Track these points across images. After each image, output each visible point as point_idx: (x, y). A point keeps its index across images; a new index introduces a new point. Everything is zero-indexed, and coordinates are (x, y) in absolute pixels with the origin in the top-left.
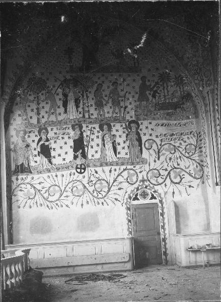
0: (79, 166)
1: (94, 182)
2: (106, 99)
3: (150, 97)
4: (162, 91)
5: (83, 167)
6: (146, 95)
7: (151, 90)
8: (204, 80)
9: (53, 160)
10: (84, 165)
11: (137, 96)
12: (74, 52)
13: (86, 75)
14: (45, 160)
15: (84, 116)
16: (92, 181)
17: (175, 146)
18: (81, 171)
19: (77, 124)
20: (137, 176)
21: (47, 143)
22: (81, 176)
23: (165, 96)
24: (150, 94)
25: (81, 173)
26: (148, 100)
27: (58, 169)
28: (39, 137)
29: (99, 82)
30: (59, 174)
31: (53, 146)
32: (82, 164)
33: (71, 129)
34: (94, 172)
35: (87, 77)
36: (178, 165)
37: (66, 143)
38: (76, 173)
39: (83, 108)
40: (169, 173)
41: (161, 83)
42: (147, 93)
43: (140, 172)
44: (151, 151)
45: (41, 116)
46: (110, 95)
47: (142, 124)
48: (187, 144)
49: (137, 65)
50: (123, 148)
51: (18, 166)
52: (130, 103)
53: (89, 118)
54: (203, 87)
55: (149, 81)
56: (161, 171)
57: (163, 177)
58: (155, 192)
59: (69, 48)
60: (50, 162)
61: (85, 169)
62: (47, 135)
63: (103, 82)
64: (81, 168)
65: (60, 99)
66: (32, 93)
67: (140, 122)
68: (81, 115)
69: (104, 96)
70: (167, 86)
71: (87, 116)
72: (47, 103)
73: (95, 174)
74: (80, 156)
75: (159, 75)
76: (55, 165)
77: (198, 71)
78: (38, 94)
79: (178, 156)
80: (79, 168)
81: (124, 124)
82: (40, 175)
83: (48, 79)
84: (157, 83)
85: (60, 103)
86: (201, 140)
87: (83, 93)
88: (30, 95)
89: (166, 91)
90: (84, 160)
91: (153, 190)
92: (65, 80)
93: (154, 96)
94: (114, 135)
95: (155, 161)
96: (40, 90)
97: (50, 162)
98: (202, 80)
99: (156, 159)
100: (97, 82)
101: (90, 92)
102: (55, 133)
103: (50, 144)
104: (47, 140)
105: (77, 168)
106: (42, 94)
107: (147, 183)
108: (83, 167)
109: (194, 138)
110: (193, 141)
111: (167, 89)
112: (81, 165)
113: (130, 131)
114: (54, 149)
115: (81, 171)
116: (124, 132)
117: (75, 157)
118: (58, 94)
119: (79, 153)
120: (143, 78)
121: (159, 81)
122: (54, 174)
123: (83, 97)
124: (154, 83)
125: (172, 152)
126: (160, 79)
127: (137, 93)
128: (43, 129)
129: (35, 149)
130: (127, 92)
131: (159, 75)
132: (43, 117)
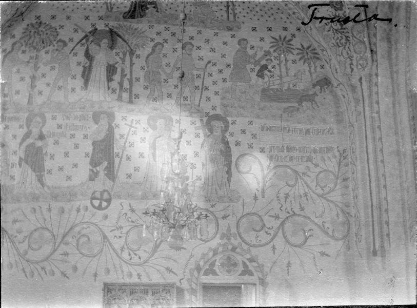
0: (98, 195)
1: (125, 230)
2: (168, 70)
3: (254, 75)
4: (277, 67)
7: (256, 63)
8: (354, 58)
9: (49, 180)
11: (227, 73)
13: (136, 26)
14: (31, 176)
16: (121, 228)
17: (296, 172)
19: (104, 113)
20: (218, 225)
21: (39, 143)
22: (101, 213)
23: (281, 77)
24: (252, 70)
25: (100, 208)
27: (55, 197)
28: (25, 130)
29: (158, 39)
30: (56, 205)
31: (50, 149)
32: (105, 191)
33: (91, 119)
34: (126, 208)
36: (302, 209)
37: (77, 147)
39: (121, 84)
40: (283, 224)
41: (276, 54)
42: (249, 67)
43: (224, 217)
46: (176, 63)
47: (234, 122)
49: (231, 17)
52: (215, 83)
55: (252, 47)
56: (266, 218)
57: (269, 231)
58: (252, 260)
60: (40, 180)
61: (109, 201)
62: (43, 126)
63: (166, 41)
64: (101, 199)
65: (79, 64)
66: (27, 49)
67: (230, 119)
72: (53, 68)
74: (102, 174)
76: (48, 187)
78: (38, 51)
83: (62, 27)
84: (267, 53)
86: (347, 165)
87: (125, 54)
88: (24, 52)
89: (284, 70)
90: (109, 183)
91: (248, 256)
92: (94, 31)
97: (40, 180)
98: (351, 58)
100: (152, 40)
101: (138, 56)
102: (60, 126)
104: (41, 137)
105: (93, 198)
106: (47, 52)
107: (235, 242)
108: (106, 196)
109: (333, 160)
110: (332, 165)
111: (286, 65)
112: (102, 193)
114: (52, 157)
117: (93, 176)
118: (75, 54)
119: (101, 169)
121: (272, 50)
124: (263, 53)
125: (291, 183)
126: (272, 47)
127: (228, 66)
128: (36, 115)
129: (15, 152)
130: (209, 62)
131: (273, 40)
132: (40, 93)
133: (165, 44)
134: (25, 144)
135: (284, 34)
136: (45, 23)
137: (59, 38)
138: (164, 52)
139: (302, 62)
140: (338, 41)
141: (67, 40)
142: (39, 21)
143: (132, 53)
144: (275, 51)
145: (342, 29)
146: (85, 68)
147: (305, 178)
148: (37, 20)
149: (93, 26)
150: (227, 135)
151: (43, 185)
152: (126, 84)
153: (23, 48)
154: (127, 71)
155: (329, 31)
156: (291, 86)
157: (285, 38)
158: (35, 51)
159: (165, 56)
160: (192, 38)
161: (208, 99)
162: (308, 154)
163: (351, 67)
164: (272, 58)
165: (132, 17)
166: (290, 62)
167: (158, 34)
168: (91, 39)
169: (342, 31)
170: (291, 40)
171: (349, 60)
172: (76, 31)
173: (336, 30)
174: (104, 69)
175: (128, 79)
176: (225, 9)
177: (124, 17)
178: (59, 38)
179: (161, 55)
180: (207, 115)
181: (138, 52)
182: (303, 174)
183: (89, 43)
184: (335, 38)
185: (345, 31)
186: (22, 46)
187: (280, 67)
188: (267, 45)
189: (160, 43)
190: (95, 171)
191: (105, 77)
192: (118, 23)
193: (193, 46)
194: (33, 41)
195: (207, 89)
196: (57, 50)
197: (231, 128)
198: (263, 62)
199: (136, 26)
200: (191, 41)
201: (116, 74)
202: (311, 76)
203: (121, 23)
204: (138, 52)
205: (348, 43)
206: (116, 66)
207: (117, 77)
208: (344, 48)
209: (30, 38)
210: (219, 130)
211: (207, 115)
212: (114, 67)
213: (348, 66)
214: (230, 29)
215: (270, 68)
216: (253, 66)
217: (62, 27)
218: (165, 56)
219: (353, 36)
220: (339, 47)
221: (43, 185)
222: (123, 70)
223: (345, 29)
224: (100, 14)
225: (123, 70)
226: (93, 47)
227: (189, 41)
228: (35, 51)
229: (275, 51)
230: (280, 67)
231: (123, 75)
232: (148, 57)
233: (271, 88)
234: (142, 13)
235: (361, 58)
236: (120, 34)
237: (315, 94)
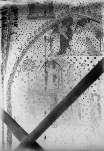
2: (76, 75)
12: (54, 41)
13: (62, 57)
15: (58, 88)
28: (28, 100)
29: (72, 63)
35: (63, 59)
39: (58, 82)
50: (86, 114)
53: (62, 89)
59: (50, 38)
62: (34, 99)
68: (57, 87)
71: (60, 87)
87: (59, 70)
94: (79, 104)
96: (31, 68)
100: (69, 63)
101: (64, 71)
106: (32, 71)
123: (59, 73)
133: (74, 65)
134: (29, 105)
136: (30, 60)
137: (35, 65)
138: (74, 68)
141: (38, 66)
142: (28, 59)
143: (62, 69)
150: (100, 102)
152: (60, 83)
154: (60, 77)
159: (74, 69)
160: (85, 61)
165: (61, 54)
174: (52, 76)
175: (61, 80)
177: (58, 54)
178: (35, 65)
181: (64, 69)
183: (46, 67)
189: (72, 65)
191: (53, 80)
193: (85, 64)
196: (35, 70)
199: (62, 57)
200: (85, 62)
201: (56, 78)
203: (57, 57)
204: (64, 69)
206: (56, 75)
207: (57, 80)
209: (26, 66)
210: (96, 100)
211: (92, 94)
212: (55, 76)
217: (35, 61)
222: (59, 77)
224: (48, 54)
225: (59, 77)
226: (47, 68)
227: (84, 62)
231: (59, 79)
232: (68, 71)
234: (65, 52)
236: (57, 62)
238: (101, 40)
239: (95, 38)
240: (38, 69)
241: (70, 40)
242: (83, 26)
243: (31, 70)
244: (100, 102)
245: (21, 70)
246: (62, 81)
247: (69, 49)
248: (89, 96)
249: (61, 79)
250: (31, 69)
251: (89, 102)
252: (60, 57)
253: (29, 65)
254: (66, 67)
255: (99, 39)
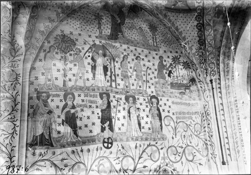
0: (106, 140)
1: (121, 159)
2: (131, 70)
4: (175, 72)
5: (110, 141)
6: (163, 73)
7: (167, 69)
9: (80, 133)
10: (111, 139)
12: (103, 19)
13: (114, 44)
14: (69, 130)
15: (111, 86)
18: (108, 145)
19: (105, 93)
20: (159, 153)
22: (108, 151)
24: (166, 73)
25: (108, 148)
26: (164, 78)
27: (84, 143)
28: (64, 103)
29: (125, 53)
31: (79, 115)
33: (99, 97)
34: (120, 148)
35: (114, 46)
36: (191, 143)
37: (93, 113)
38: (103, 148)
39: (111, 77)
40: (184, 150)
41: (174, 65)
42: (165, 71)
43: (162, 149)
44: (169, 127)
45: (67, 79)
46: (134, 67)
48: (195, 123)
50: (147, 123)
51: (37, 137)
52: (151, 79)
53: (116, 88)
54: (207, 75)
55: (165, 61)
56: (178, 148)
57: (180, 154)
58: (174, 170)
60: (75, 133)
61: (112, 143)
62: (73, 101)
64: (108, 143)
65: (89, 64)
66: (59, 51)
67: (159, 98)
68: (109, 84)
69: (129, 68)
70: (179, 69)
71: (114, 84)
72: (75, 65)
73: (122, 150)
74: (107, 128)
75: (173, 58)
76: (80, 137)
77: (203, 61)
79: (190, 134)
80: (106, 142)
81: (146, 98)
82: (63, 150)
84: (171, 65)
85: (89, 68)
86: (204, 121)
88: (57, 53)
90: (111, 133)
91: (173, 168)
93: (169, 76)
94: (138, 109)
95: (173, 138)
96: (69, 50)
97: (75, 133)
99: (174, 136)
101: (117, 62)
102: (83, 101)
103: (77, 112)
104: (73, 107)
105: (104, 142)
106: (71, 55)
107: (167, 161)
108: (110, 141)
110: (199, 120)
111: (178, 71)
112: (108, 139)
113: (151, 105)
114: (81, 119)
115: (108, 145)
116: (147, 106)
117: (103, 129)
119: (106, 125)
120: (161, 58)
121: (173, 63)
122: (79, 148)
125: (185, 130)
126: (172, 61)
128: (69, 94)
129: (59, 117)
131: (173, 58)
132: (70, 80)
135: (176, 55)
139: (184, 69)
140: (201, 61)
143: (114, 60)
144: (174, 63)
145: (202, 55)
146: (92, 66)
147: (190, 127)
148: (62, 33)
149: (94, 41)
150: (159, 106)
151: (77, 136)
152: (113, 78)
153: (56, 50)
154: (113, 70)
155: (197, 55)
156: (181, 81)
157: (177, 57)
158: (64, 53)
160: (140, 54)
161: (150, 87)
162: (190, 115)
163: (206, 74)
164: (173, 67)
165: (112, 39)
166: (180, 70)
167: (125, 50)
168: (94, 49)
169: (203, 56)
170: (179, 58)
171: (205, 70)
172: (85, 43)
173: (200, 55)
174: (102, 68)
175: (114, 75)
176: (152, 39)
177: (108, 38)
179: (127, 62)
180: (150, 96)
182: (189, 125)
184: (200, 59)
185: (204, 56)
186: (55, 49)
187: (176, 72)
188: (170, 61)
190: (104, 127)
192: (106, 41)
194: (62, 47)
195: (148, 82)
196: (76, 54)
197: (160, 103)
198: (170, 69)
199: (114, 44)
200: (139, 55)
201: (108, 71)
202: (188, 77)
203: (107, 42)
204: (117, 59)
205: (205, 63)
206: (108, 66)
207: (109, 73)
208: (204, 65)
209: (60, 44)
210: (155, 104)
211: (150, 96)
212: (107, 67)
213: (205, 73)
214: (155, 51)
215: (172, 72)
216: (166, 71)
218: (129, 62)
219: (209, 59)
220: (201, 64)
221: (77, 136)
222: (111, 69)
223: (204, 55)
225: (111, 69)
228: (64, 53)
229: (174, 64)
230: (176, 72)
231: (111, 73)
233: (174, 82)
234: (116, 37)
235: (213, 71)
236: (108, 48)
237: (190, 86)
238: (154, 34)
239: (148, 30)
240: (80, 53)
241: (123, 25)
242: (136, 13)
243: (69, 53)
244: (159, 106)
245: (51, 49)
246: (115, 75)
247: (121, 36)
248: (148, 98)
249: (114, 73)
250: (69, 52)
251: (149, 106)
252: (111, 43)
253: (66, 44)
254: (119, 57)
255: (152, 32)
